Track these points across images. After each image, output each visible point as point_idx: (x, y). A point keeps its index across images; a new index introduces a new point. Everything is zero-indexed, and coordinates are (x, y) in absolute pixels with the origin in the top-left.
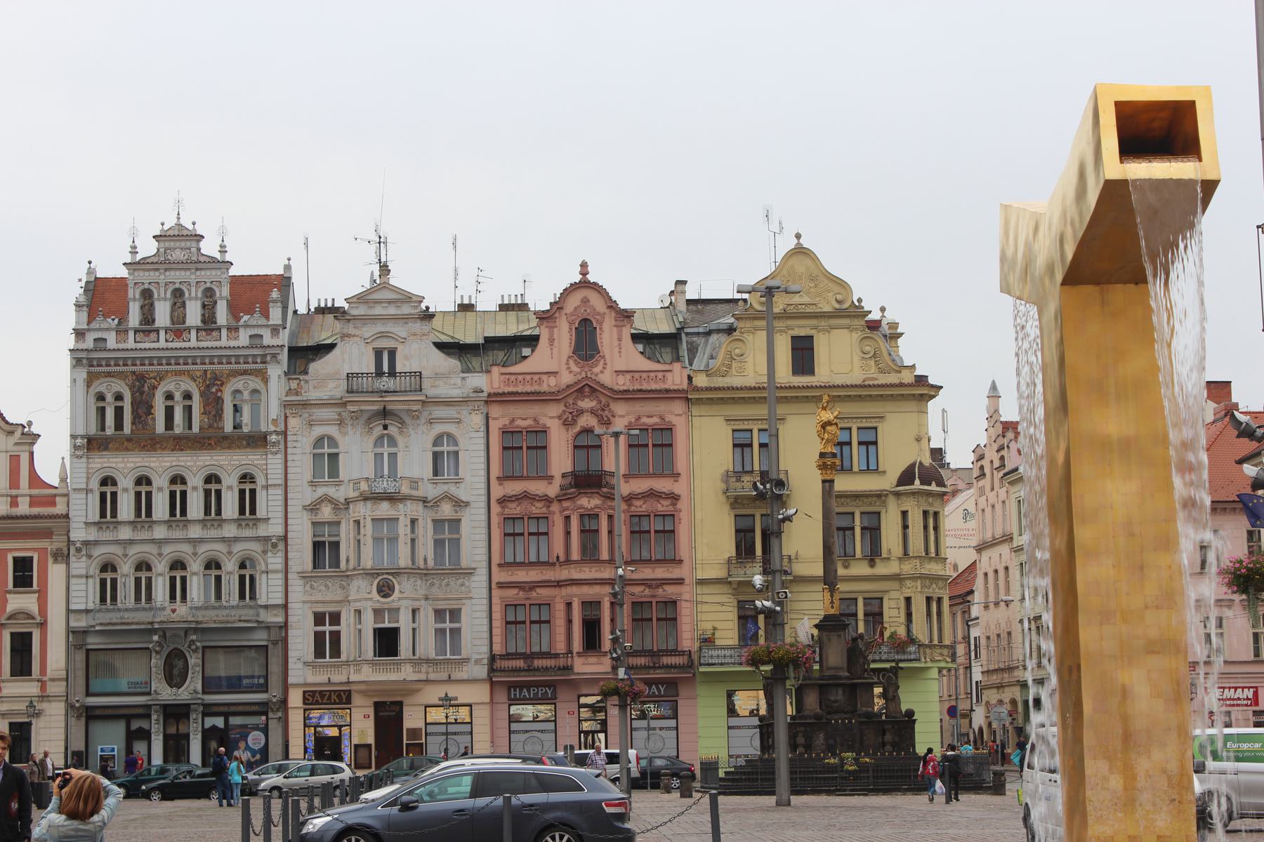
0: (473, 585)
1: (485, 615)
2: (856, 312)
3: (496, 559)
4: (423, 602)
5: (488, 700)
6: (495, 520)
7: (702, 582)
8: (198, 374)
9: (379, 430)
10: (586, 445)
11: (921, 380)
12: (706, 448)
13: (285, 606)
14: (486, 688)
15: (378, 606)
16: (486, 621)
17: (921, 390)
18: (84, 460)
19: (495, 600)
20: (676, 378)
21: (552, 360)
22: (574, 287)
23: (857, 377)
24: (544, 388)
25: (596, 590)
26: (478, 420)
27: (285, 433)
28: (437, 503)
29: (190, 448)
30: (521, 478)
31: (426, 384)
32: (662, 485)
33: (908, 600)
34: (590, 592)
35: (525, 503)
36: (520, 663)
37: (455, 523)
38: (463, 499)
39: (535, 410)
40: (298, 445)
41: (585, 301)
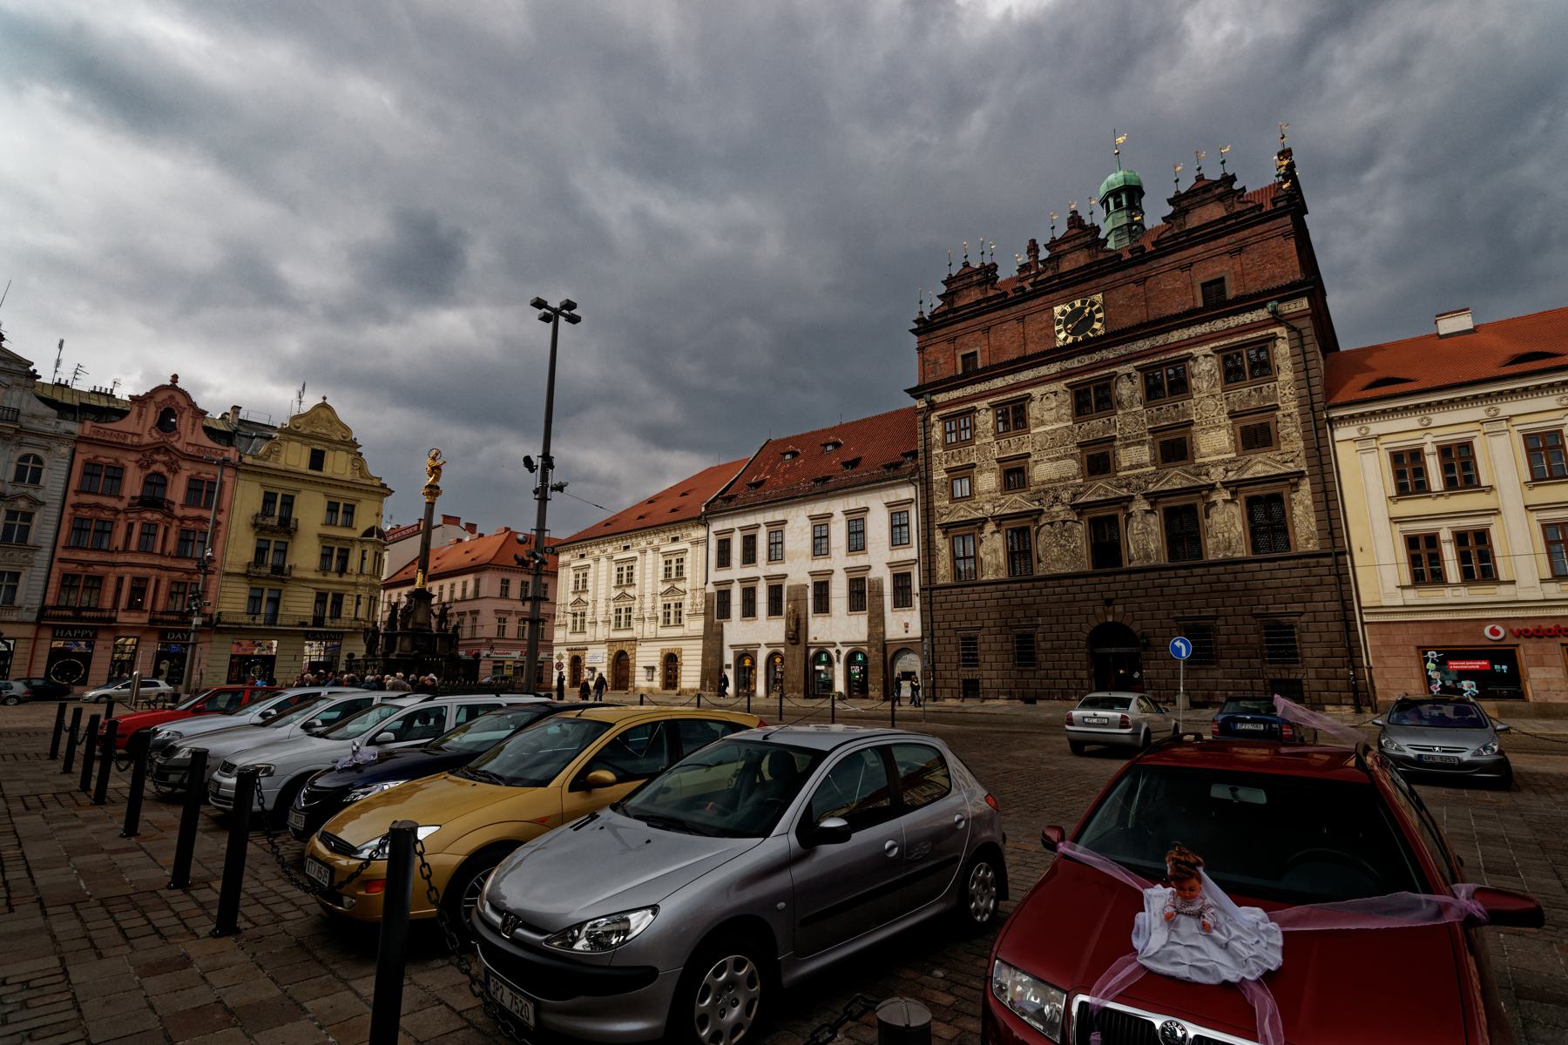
2: (353, 444)
6: (66, 517)
7: (228, 574)
10: (155, 483)
11: (383, 486)
12: (245, 499)
17: (383, 491)
20: (232, 454)
21: (142, 428)
22: (162, 388)
23: (348, 477)
24: (128, 441)
26: (65, 450)
28: (14, 498)
30: (96, 494)
31: (21, 419)
32: (210, 514)
33: (359, 597)
34: (139, 571)
36: (70, 613)
37: (28, 517)
39: (118, 454)
41: (172, 397)
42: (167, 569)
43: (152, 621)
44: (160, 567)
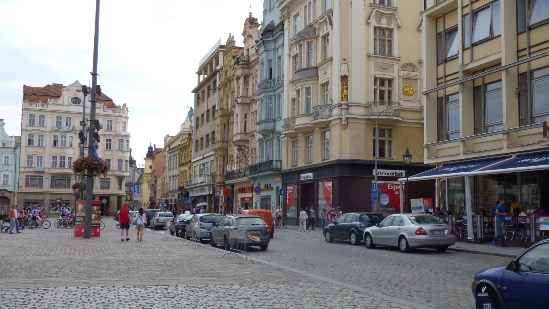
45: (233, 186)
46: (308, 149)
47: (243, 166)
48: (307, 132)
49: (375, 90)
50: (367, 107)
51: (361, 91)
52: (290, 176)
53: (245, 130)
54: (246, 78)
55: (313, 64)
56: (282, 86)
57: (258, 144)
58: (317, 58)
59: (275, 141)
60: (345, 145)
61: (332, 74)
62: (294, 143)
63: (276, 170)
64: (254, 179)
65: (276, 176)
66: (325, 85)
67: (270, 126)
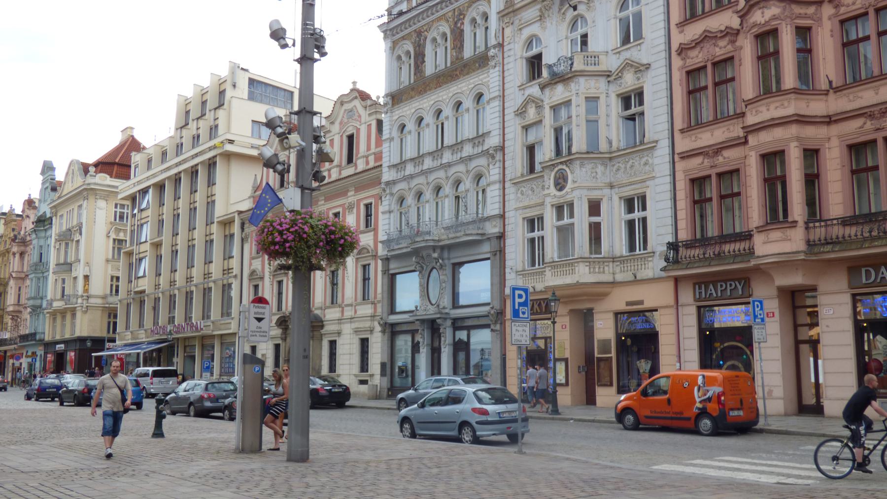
0: (656, 161)
1: (668, 195)
3: (679, 124)
4: (607, 191)
5: (671, 301)
8: (450, 14)
9: (571, 13)
13: (503, 216)
14: (668, 288)
15: (556, 201)
16: (669, 204)
18: (388, 114)
19: (680, 176)
25: (778, 133)
27: (501, 46)
29: (446, 83)
34: (767, 140)
35: (707, 45)
38: (645, 62)
40: (512, 53)
42: (829, 120)
43: (808, 243)
44: (801, 120)
45: (5, 352)
46: (63, 326)
47: (16, 335)
48: (63, 313)
49: (112, 286)
50: (104, 297)
51: (99, 286)
52: (49, 346)
53: (19, 301)
54: (22, 254)
55: (69, 261)
56: (48, 271)
57: (28, 317)
58: (71, 258)
59: (41, 315)
60: (85, 326)
61: (79, 271)
62: (55, 319)
63: (40, 340)
64: (24, 347)
65: (40, 345)
66: (75, 278)
67: (38, 302)
